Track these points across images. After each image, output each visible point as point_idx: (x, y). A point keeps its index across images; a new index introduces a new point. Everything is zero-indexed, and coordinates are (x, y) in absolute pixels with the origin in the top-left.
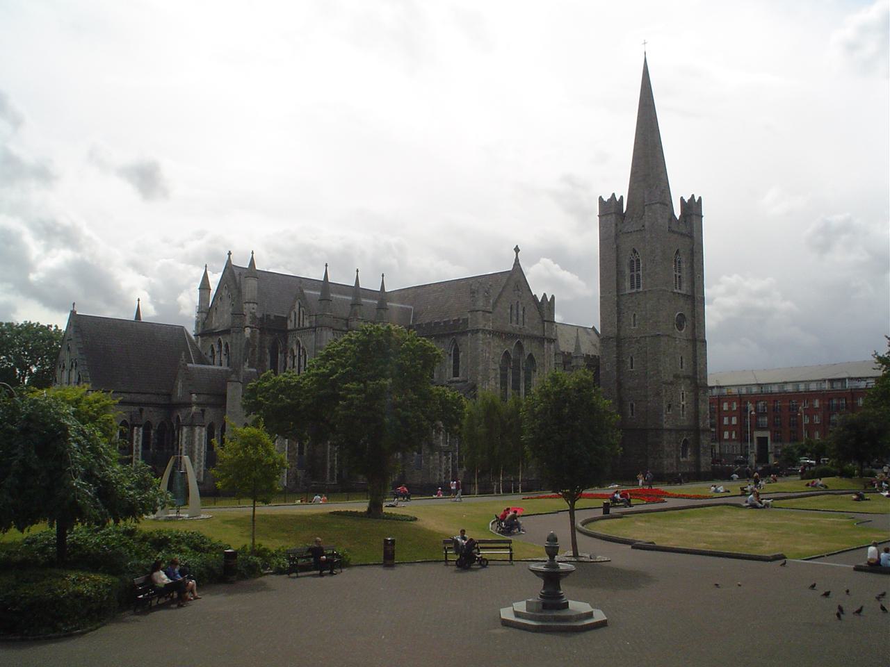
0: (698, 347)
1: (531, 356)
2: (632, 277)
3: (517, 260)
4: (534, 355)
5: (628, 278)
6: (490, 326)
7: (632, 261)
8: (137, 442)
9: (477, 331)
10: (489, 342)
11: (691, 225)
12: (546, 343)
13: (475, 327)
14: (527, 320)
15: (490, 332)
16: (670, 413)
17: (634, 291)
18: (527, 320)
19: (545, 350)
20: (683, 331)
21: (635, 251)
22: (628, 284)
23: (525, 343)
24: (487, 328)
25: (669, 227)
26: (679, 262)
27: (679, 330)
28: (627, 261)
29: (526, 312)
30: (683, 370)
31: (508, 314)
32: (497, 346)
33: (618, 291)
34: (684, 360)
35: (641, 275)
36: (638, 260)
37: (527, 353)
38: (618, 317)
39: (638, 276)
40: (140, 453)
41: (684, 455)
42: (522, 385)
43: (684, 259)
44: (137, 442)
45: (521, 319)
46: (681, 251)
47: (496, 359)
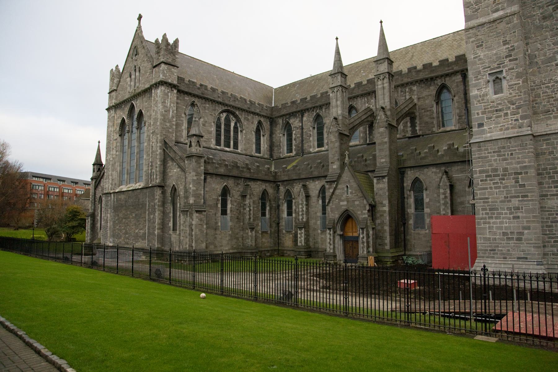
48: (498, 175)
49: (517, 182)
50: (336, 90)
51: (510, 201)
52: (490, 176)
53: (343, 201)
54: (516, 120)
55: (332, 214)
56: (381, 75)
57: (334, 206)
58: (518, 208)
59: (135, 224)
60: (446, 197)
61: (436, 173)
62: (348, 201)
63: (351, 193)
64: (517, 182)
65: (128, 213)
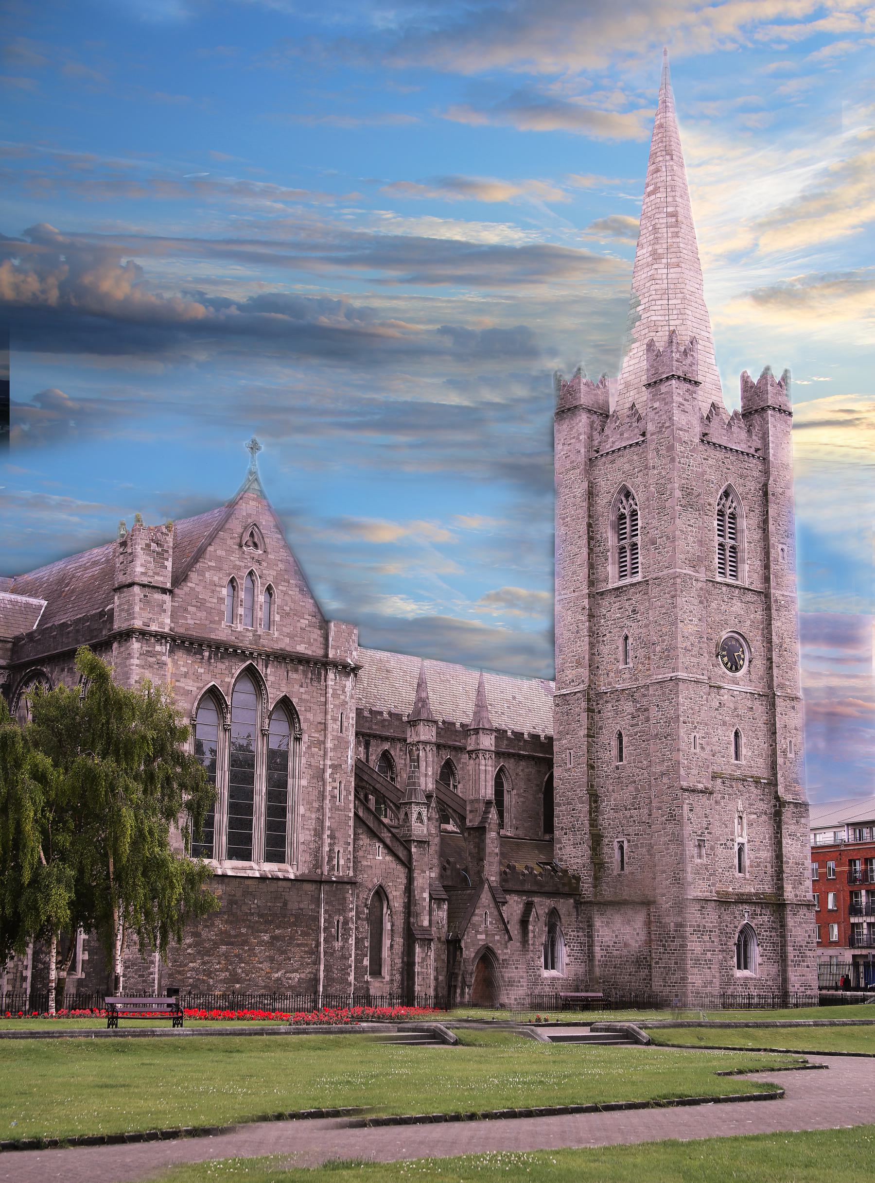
0: (778, 709)
1: (286, 705)
2: (622, 550)
4: (295, 701)
5: (612, 556)
6: (164, 623)
7: (622, 517)
9: (126, 635)
11: (765, 437)
12: (331, 675)
13: (124, 626)
14: (277, 618)
15: (160, 637)
16: (705, 860)
17: (628, 581)
18: (277, 618)
19: (330, 691)
20: (739, 674)
21: (628, 495)
22: (612, 569)
23: (269, 670)
24: (154, 628)
25: (705, 435)
26: (733, 516)
27: (730, 669)
28: (613, 518)
30: (743, 762)
31: (221, 600)
32: (186, 675)
33: (591, 583)
34: (743, 740)
35: (639, 546)
36: (634, 513)
37: (274, 694)
38: (592, 645)
39: (634, 546)
41: (743, 962)
42: (261, 772)
43: (743, 509)
45: (259, 614)
46: (739, 490)
48: (699, 931)
49: (710, 938)
50: (428, 748)
51: (706, 954)
52: (695, 931)
53: (481, 933)
54: (709, 886)
55: (467, 952)
56: (487, 753)
57: (469, 940)
58: (710, 960)
59: (271, 959)
60: (534, 937)
61: (517, 902)
62: (487, 935)
63: (491, 923)
64: (710, 938)
65: (244, 931)
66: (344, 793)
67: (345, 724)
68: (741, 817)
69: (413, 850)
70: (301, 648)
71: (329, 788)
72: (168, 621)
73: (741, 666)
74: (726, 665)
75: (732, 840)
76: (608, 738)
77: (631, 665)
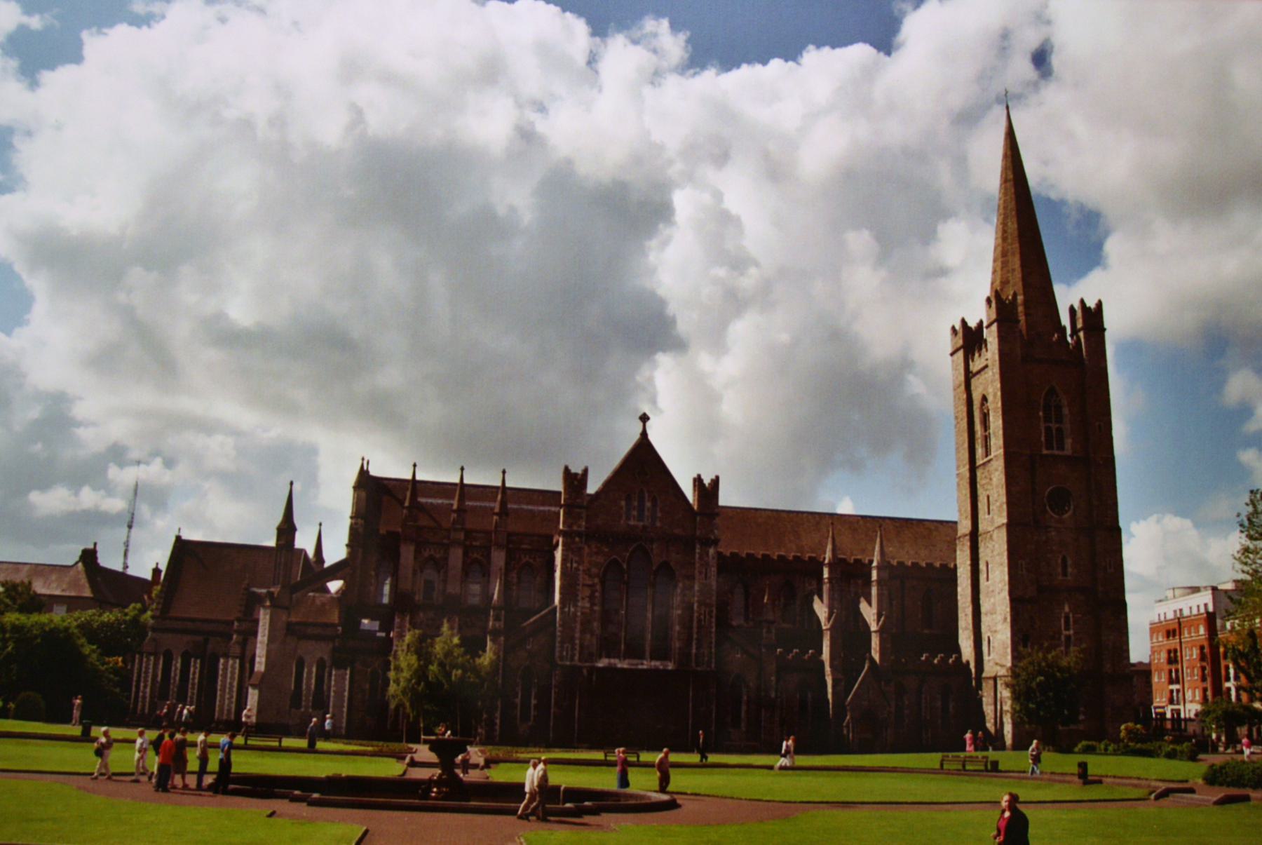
3: (644, 434)
8: (194, 673)
10: (580, 549)
12: (698, 546)
14: (659, 515)
15: (579, 534)
18: (659, 515)
19: (697, 556)
20: (1066, 516)
21: (984, 399)
23: (654, 547)
29: (659, 502)
34: (1069, 562)
39: (989, 434)
40: (196, 687)
44: (194, 673)
47: (594, 570)
66: (707, 617)
67: (709, 575)
68: (1067, 618)
69: (763, 650)
70: (677, 531)
71: (696, 615)
72: (584, 523)
73: (1067, 512)
74: (1053, 510)
75: (1060, 633)
76: (982, 566)
77: (991, 515)
